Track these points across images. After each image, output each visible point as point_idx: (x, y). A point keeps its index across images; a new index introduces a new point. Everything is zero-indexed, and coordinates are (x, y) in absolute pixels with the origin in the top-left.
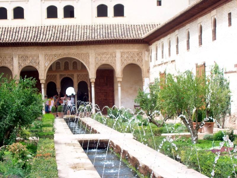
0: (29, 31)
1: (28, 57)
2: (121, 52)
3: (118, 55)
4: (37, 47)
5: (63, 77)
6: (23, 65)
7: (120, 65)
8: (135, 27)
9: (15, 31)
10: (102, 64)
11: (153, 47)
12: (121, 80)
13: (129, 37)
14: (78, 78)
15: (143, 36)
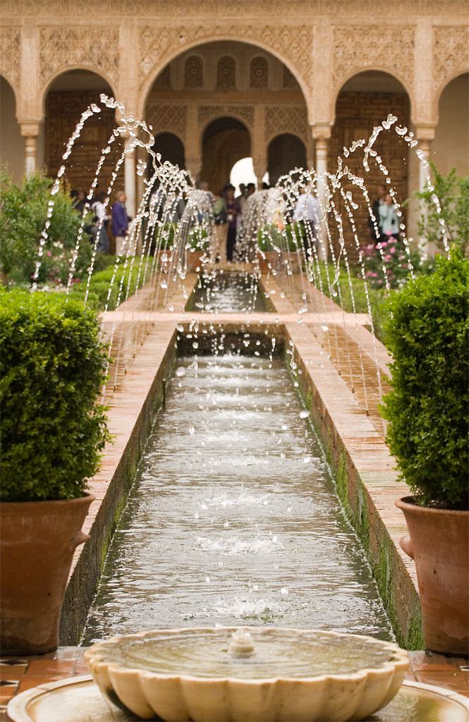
1: (75, 37)
2: (433, 26)
3: (424, 37)
6: (58, 68)
7: (430, 77)
10: (361, 71)
12: (430, 134)
14: (271, 121)
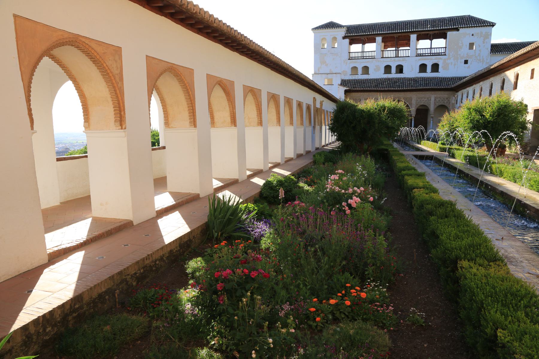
3: (433, 99)
11: (460, 93)
15: (452, 86)
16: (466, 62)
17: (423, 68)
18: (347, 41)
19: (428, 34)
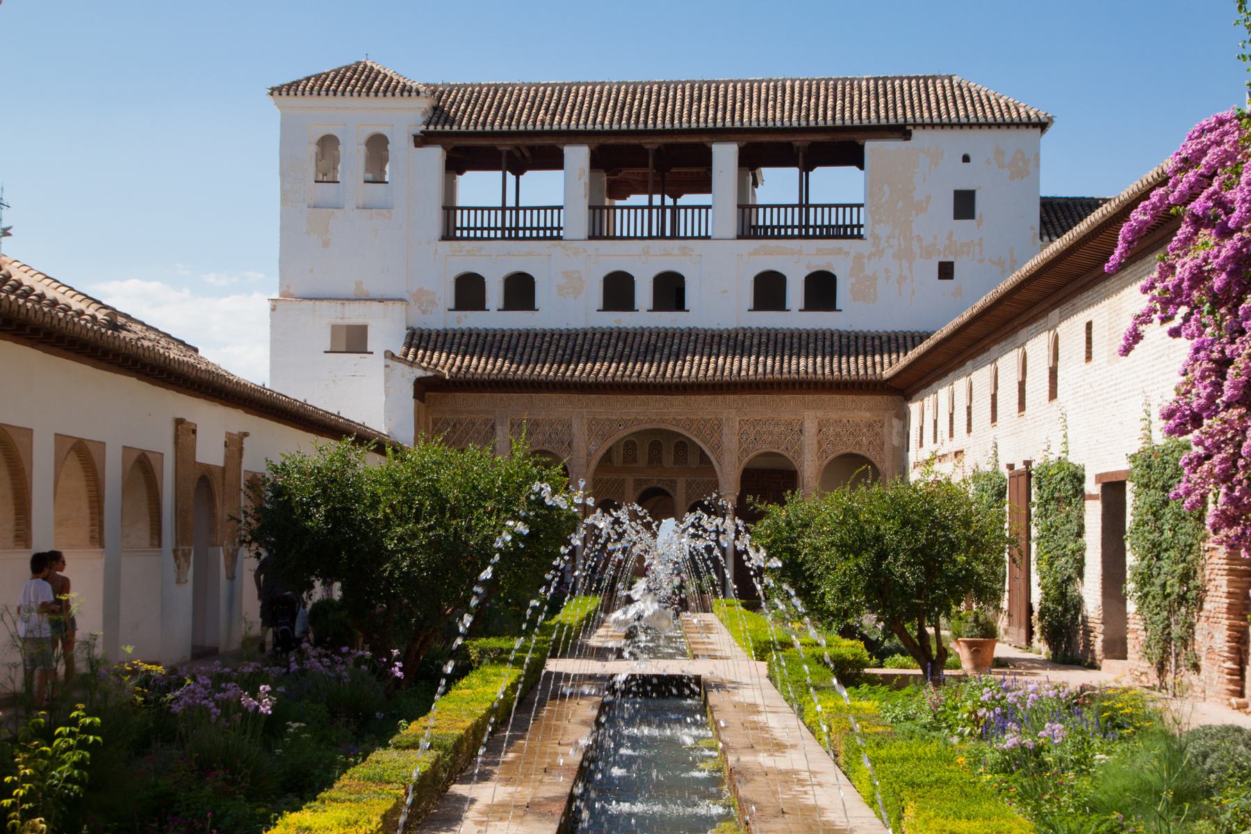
0: (545, 345)
3: (810, 427)
4: (565, 396)
5: (644, 487)
8: (869, 343)
9: (504, 346)
11: (914, 408)
13: (844, 372)
15: (888, 373)
16: (946, 271)
17: (769, 290)
18: (435, 155)
19: (789, 144)
